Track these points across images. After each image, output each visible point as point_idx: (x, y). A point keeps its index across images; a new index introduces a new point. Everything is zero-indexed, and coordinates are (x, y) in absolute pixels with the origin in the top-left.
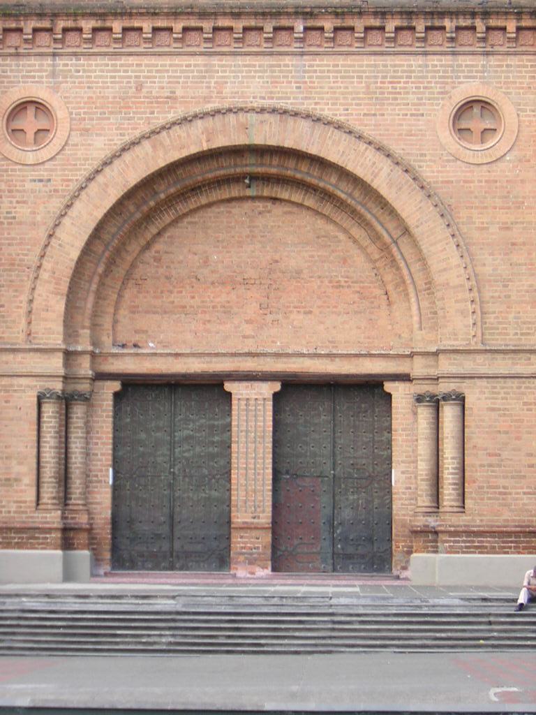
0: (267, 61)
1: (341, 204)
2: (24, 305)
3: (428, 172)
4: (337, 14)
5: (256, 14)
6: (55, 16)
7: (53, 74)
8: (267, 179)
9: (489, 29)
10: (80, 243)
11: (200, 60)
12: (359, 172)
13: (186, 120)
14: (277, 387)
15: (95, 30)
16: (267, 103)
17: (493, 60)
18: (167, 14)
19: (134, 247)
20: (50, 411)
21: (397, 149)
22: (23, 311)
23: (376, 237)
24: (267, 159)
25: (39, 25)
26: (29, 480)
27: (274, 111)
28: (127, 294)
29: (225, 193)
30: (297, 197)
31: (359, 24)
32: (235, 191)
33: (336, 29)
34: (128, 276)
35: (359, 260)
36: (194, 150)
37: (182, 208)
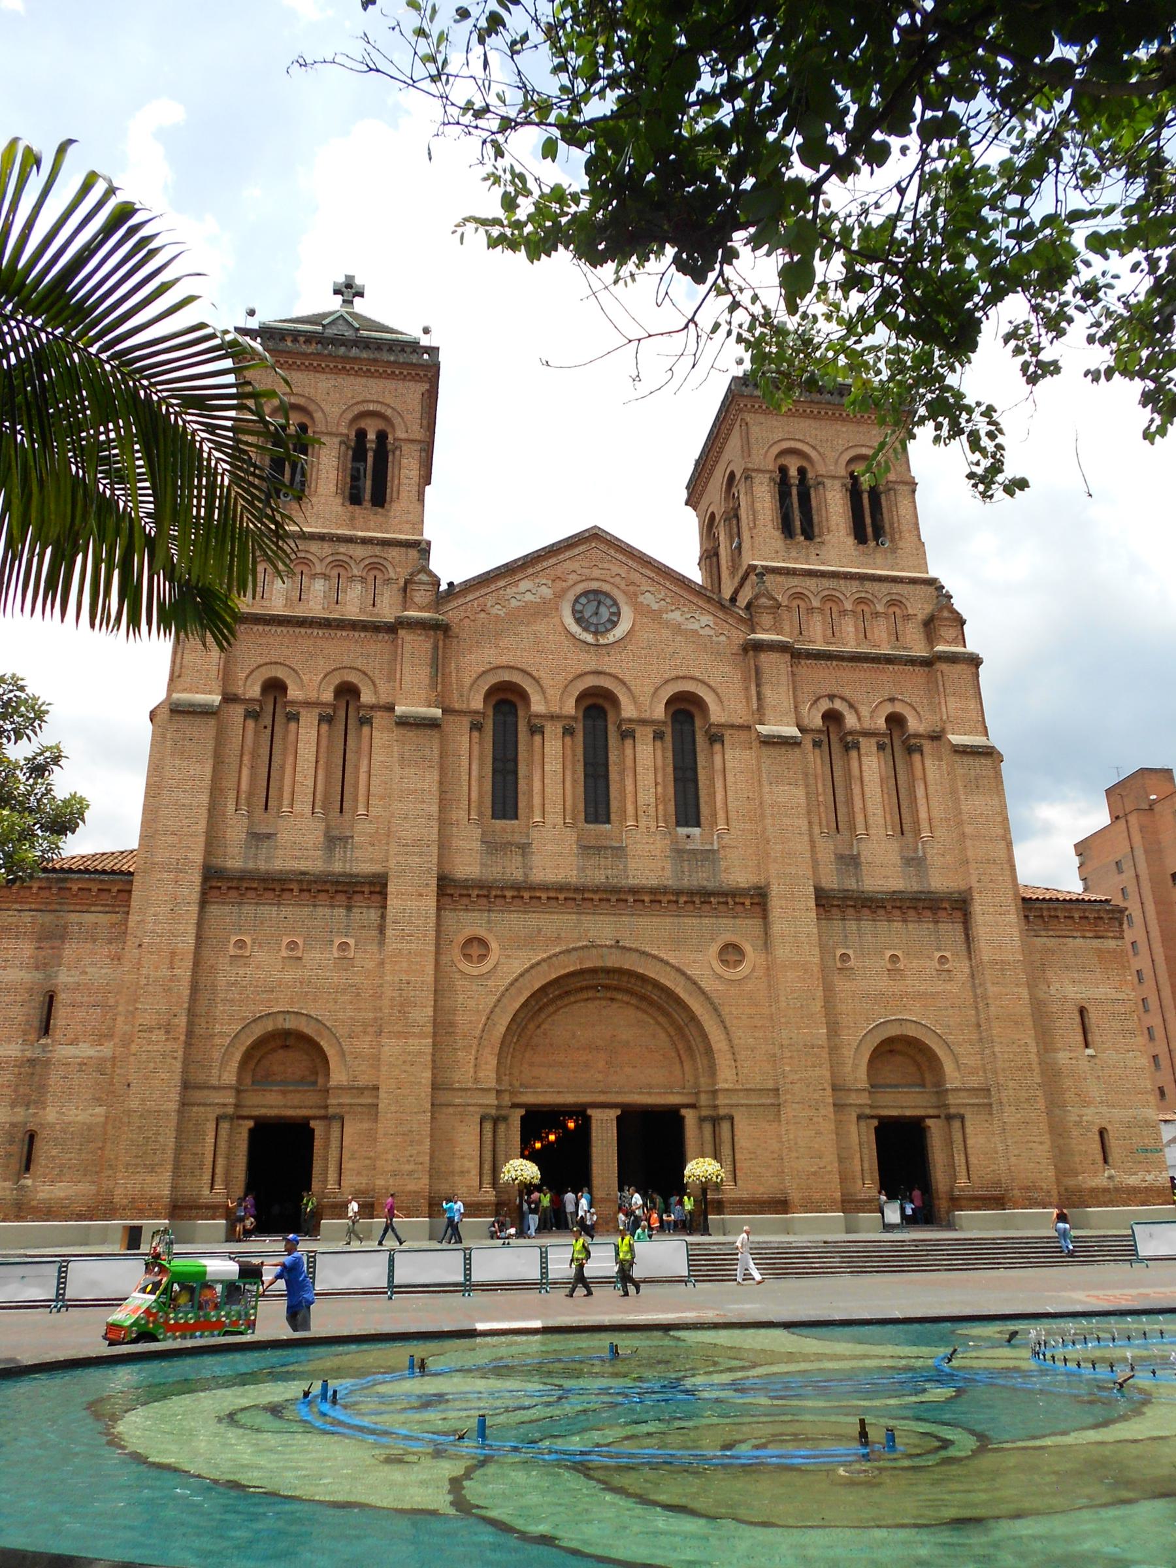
0: (612, 918)
1: (652, 1003)
2: (473, 1061)
5: (605, 891)
7: (489, 922)
8: (606, 987)
11: (574, 917)
13: (568, 951)
14: (619, 1112)
17: (738, 921)
19: (531, 1026)
20: (488, 1126)
22: (472, 1064)
23: (673, 1022)
24: (611, 975)
26: (475, 1172)
29: (585, 995)
30: (626, 998)
31: (665, 899)
32: (591, 994)
35: (663, 1035)
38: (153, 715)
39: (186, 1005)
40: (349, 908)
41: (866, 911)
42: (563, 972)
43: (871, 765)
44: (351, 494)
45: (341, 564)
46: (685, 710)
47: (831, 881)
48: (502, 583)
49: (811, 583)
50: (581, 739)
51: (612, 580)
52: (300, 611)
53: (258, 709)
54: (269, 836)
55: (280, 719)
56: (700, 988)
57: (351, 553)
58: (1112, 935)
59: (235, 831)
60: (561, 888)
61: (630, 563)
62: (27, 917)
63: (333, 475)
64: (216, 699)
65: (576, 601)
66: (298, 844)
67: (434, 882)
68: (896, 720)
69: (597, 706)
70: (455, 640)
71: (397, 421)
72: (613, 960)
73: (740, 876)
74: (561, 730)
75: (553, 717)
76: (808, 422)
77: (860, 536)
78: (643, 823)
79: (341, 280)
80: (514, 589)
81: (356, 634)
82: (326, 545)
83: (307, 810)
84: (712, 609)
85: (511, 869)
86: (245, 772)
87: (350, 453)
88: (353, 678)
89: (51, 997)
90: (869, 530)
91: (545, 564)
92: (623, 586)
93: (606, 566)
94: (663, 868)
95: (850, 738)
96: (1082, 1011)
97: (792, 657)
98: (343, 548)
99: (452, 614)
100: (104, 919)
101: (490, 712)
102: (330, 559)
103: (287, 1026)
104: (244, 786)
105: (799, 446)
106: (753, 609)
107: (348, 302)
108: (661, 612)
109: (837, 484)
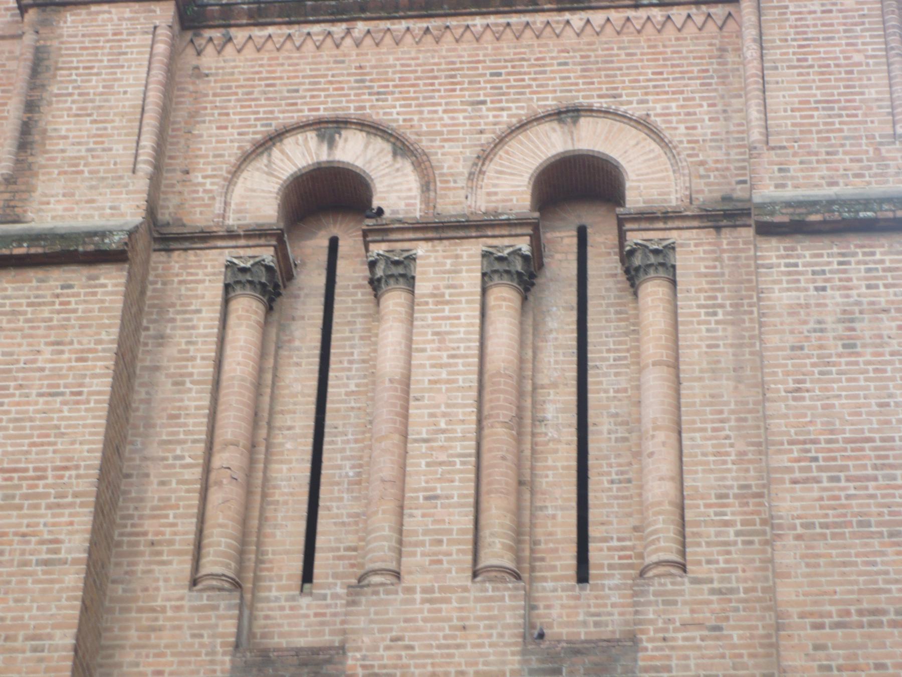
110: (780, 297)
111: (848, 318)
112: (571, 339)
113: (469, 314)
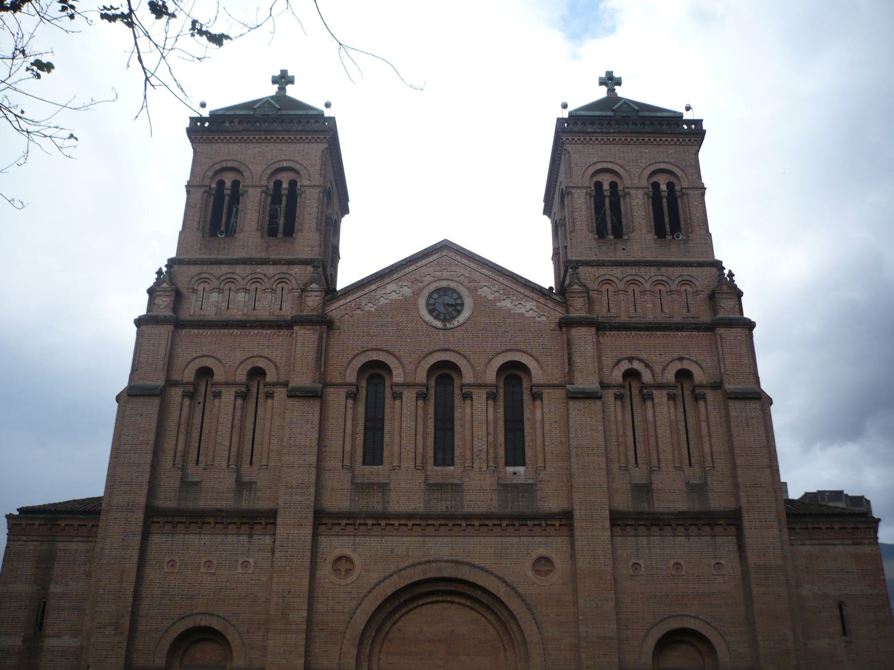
0: (449, 539)
1: (483, 604)
3: (521, 590)
4: (480, 519)
6: (356, 518)
7: (354, 544)
9: (547, 525)
10: (364, 622)
11: (420, 539)
12: (491, 590)
13: (414, 565)
15: (373, 525)
16: (450, 558)
17: (550, 539)
18: (406, 518)
19: (389, 624)
21: (508, 579)
23: (499, 619)
25: (348, 522)
27: (452, 561)
28: (385, 646)
30: (463, 601)
31: (490, 523)
33: (480, 525)
34: (386, 637)
36: (417, 579)
37: (410, 606)
38: (118, 398)
39: (130, 609)
40: (250, 536)
41: (655, 529)
42: (409, 582)
43: (662, 412)
44: (269, 229)
45: (256, 281)
46: (513, 373)
47: (624, 504)
48: (373, 287)
49: (618, 272)
50: (433, 401)
51: (458, 279)
52: (227, 316)
53: (192, 390)
54: (196, 483)
55: (209, 396)
56: (517, 592)
57: (265, 272)
58: (867, 541)
59: (169, 480)
60: (410, 516)
61: (472, 265)
62: (31, 546)
63: (255, 216)
64: (161, 383)
65: (430, 296)
66: (217, 490)
67: (311, 516)
68: (684, 375)
69: (444, 373)
70: (338, 331)
71: (303, 173)
72: (450, 572)
73: (554, 504)
74: (414, 396)
75: (408, 385)
76: (617, 147)
77: (660, 232)
78: (476, 466)
79: (277, 73)
80: (383, 291)
81: (265, 332)
82: (247, 267)
83: (224, 464)
84: (535, 296)
85: (374, 503)
86: (182, 437)
87: (270, 198)
88: (261, 363)
89: (45, 603)
90: (668, 227)
91: (407, 270)
92: (466, 283)
93: (453, 268)
94: (491, 500)
95: (645, 391)
96: (841, 606)
97: (598, 330)
98: (259, 269)
99: (335, 310)
100: (81, 547)
101: (364, 384)
102: (250, 277)
103: (203, 624)
104: (180, 447)
105: (610, 166)
106: (567, 295)
107: (282, 89)
108: (495, 300)
109: (640, 193)
110: (733, 414)
111: (747, 419)
112: (682, 410)
113: (666, 408)
